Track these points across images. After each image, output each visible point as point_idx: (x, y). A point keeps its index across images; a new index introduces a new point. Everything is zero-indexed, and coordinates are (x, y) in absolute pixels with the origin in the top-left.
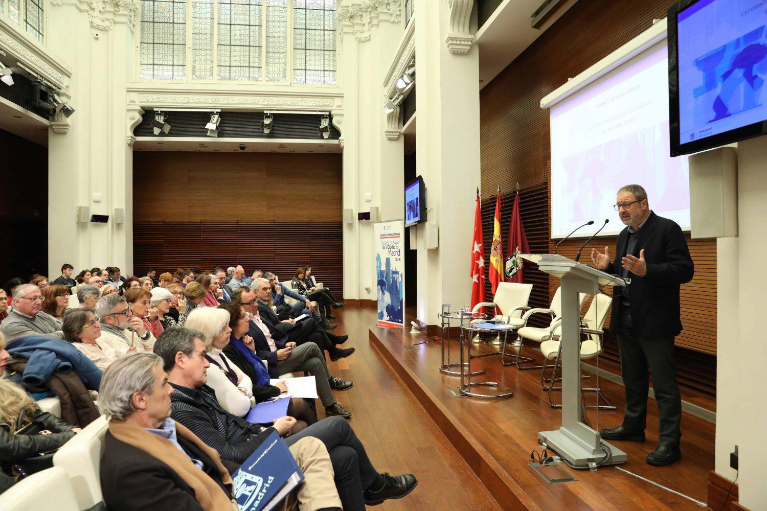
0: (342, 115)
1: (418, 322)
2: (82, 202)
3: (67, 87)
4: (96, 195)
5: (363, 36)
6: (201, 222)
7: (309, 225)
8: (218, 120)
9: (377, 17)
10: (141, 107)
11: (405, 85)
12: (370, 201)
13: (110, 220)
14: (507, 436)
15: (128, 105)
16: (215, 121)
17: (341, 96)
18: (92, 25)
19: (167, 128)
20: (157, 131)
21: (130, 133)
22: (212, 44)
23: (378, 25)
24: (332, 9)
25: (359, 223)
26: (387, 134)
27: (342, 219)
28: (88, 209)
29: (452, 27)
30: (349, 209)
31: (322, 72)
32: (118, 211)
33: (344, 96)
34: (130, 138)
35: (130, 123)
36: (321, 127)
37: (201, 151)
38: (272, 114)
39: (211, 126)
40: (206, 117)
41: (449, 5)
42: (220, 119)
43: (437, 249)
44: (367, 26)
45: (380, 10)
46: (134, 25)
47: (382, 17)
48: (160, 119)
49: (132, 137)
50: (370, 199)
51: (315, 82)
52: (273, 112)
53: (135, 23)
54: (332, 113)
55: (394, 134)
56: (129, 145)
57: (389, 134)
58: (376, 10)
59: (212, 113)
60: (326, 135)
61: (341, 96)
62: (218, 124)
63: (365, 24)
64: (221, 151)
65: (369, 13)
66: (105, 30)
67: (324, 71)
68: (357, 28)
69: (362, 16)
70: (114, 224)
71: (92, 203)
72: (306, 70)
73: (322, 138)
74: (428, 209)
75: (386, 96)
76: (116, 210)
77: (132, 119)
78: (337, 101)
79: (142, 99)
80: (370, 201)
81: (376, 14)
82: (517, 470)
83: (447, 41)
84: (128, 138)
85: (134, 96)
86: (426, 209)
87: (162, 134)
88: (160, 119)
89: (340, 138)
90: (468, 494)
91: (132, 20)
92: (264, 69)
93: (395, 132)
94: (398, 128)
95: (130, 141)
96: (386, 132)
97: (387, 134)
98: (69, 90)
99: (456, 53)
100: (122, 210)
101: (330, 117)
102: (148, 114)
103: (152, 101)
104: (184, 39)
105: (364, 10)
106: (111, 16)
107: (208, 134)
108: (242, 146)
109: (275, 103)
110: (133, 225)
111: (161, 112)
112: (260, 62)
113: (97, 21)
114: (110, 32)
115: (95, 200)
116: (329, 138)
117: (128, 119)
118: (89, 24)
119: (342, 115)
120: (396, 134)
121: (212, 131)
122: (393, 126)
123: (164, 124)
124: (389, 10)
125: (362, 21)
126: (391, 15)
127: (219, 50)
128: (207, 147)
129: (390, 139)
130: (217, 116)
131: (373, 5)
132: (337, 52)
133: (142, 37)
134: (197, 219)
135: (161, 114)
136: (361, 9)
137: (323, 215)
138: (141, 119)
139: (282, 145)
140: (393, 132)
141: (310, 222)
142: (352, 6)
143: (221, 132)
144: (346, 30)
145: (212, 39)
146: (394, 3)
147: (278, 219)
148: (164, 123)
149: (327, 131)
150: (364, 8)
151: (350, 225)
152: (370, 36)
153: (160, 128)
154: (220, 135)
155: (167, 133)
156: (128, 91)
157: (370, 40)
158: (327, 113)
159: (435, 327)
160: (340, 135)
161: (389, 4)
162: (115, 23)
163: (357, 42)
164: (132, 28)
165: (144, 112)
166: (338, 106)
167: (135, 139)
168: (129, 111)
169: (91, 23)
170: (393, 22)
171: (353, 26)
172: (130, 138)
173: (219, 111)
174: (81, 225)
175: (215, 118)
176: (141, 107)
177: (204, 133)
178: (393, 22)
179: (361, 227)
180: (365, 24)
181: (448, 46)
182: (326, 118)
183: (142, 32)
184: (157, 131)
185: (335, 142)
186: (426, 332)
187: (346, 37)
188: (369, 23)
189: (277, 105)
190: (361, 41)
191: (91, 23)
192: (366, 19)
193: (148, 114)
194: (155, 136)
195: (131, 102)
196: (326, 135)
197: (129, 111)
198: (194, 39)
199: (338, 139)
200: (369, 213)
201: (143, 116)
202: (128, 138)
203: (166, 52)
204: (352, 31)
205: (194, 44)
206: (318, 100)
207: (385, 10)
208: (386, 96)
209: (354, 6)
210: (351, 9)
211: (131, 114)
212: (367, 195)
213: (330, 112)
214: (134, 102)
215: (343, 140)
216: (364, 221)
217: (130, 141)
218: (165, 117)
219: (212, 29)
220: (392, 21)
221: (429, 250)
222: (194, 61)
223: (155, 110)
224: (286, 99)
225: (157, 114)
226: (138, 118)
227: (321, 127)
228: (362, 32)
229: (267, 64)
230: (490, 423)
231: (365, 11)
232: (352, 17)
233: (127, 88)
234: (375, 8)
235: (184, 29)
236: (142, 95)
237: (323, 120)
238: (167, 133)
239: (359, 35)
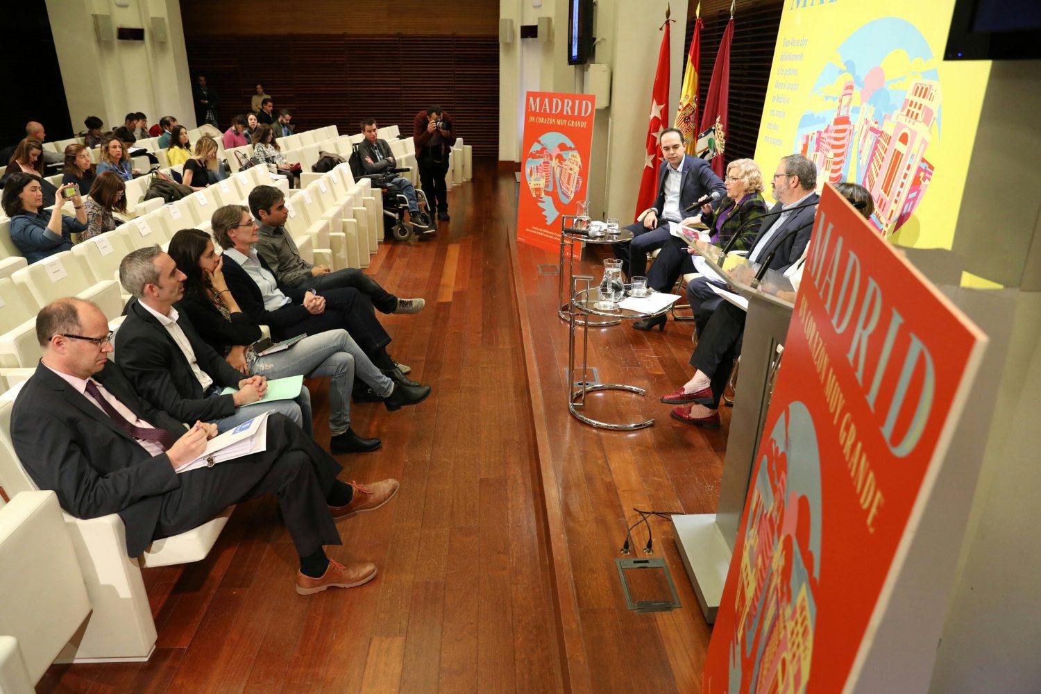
13: (147, 36)
14: (611, 488)
25: (523, 42)
28: (108, 18)
30: (506, 20)
32: (157, 21)
43: (608, 109)
71: (116, 9)
74: (598, 40)
80: (540, 6)
82: (592, 571)
86: (595, 39)
90: (517, 588)
100: (163, 19)
110: (186, 41)
134: (283, 30)
151: (510, 46)
216: (530, 40)
230: (598, 453)
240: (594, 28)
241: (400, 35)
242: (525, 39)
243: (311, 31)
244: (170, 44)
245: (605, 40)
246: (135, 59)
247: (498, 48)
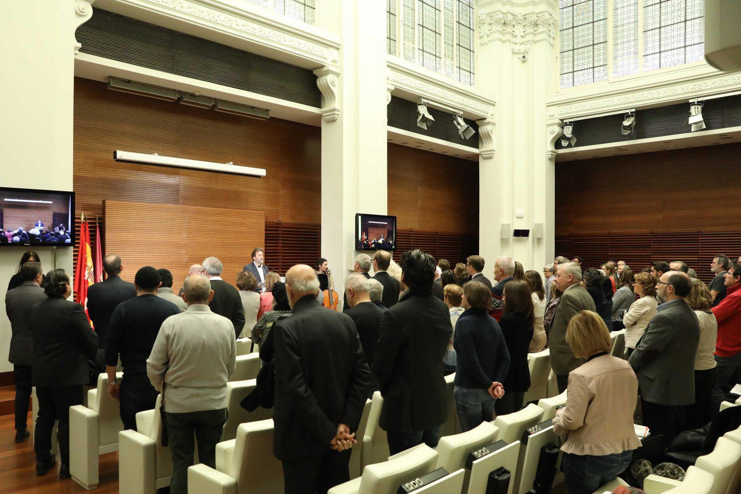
2: (505, 220)
3: (492, 115)
4: (519, 211)
15: (548, 120)
21: (551, 147)
32: (539, 226)
40: (622, 117)
46: (553, 38)
71: (516, 220)
76: (535, 224)
91: (551, 34)
98: (494, 117)
100: (542, 225)
145: (636, 28)
156: (547, 106)
162: (535, 42)
168: (548, 126)
173: (633, 110)
174: (504, 241)
197: (548, 126)
211: (551, 129)
214: (553, 116)
217: (550, 155)
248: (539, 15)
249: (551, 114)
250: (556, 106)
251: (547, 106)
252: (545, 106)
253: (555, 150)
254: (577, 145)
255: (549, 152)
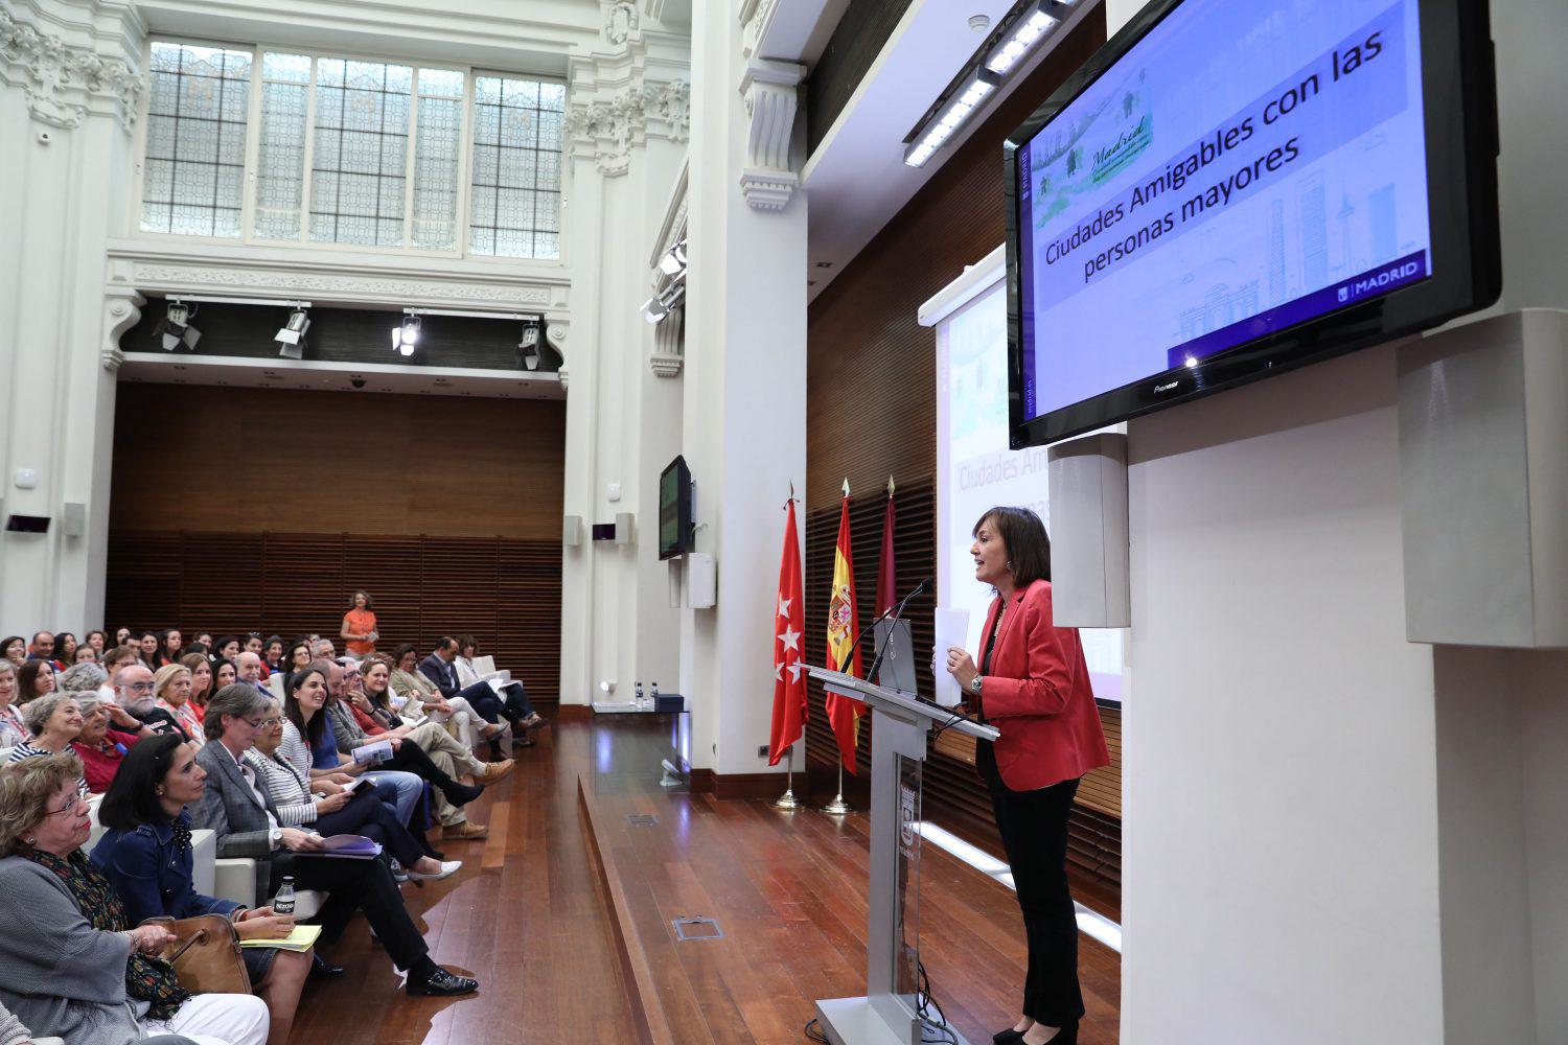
0: (566, 323)
1: (678, 762)
4: (24, 473)
5: (615, 165)
6: (266, 535)
7: (496, 546)
8: (303, 325)
9: (643, 129)
10: (139, 291)
11: (679, 268)
12: (618, 500)
13: (52, 528)
16: (297, 325)
17: (565, 284)
18: (33, 114)
19: (193, 337)
20: (169, 341)
21: (110, 345)
22: (300, 169)
23: (643, 145)
24: (555, 109)
25: (595, 545)
26: (655, 364)
27: (561, 535)
29: (752, 157)
31: (530, 235)
32: (74, 510)
33: (572, 283)
34: (111, 356)
35: (112, 323)
36: (521, 346)
37: (271, 386)
38: (419, 315)
39: (288, 336)
40: (281, 316)
41: (747, 111)
42: (308, 322)
43: (714, 609)
44: (623, 147)
45: (648, 114)
46: (132, 121)
47: (651, 129)
48: (179, 318)
49: (114, 353)
50: (616, 496)
51: (515, 251)
52: (421, 312)
53: (134, 117)
54: (546, 317)
55: (668, 364)
56: (108, 369)
57: (659, 364)
58: (642, 115)
59: (293, 310)
60: (531, 363)
61: (565, 284)
62: (303, 334)
63: (618, 142)
64: (314, 387)
65: (626, 120)
66: (64, 127)
67: (534, 231)
68: (602, 148)
69: (613, 125)
70: (64, 538)
71: (13, 491)
72: (495, 228)
73: (525, 368)
74: (697, 526)
75: (654, 287)
76: (68, 505)
77: (116, 315)
78: (558, 294)
79: (140, 274)
80: (618, 500)
81: (641, 122)
83: (743, 183)
84: (105, 355)
85: (123, 268)
86: (694, 524)
87: (181, 349)
88: (179, 318)
89: (560, 369)
91: (129, 110)
92: (408, 224)
93: (671, 361)
94: (679, 354)
95: (109, 361)
96: (653, 360)
97: (655, 364)
99: (760, 209)
100: (82, 506)
101: (542, 325)
102: (153, 306)
103: (161, 279)
104: (241, 155)
105: (617, 113)
106: (79, 99)
107: (282, 353)
108: (358, 380)
109: (426, 294)
111: (182, 302)
112: (401, 208)
113: (45, 108)
114: (75, 133)
115: (20, 482)
116: (537, 370)
117: (108, 316)
118: (26, 114)
119: (566, 323)
120: (673, 365)
121: (290, 346)
122: (668, 347)
123: (186, 328)
124: (667, 116)
125: (613, 134)
126: (671, 125)
127: (315, 181)
128: (279, 378)
129: (660, 376)
130: (301, 316)
131: (634, 105)
132: (563, 197)
133: (150, 145)
134: (258, 528)
135: (181, 308)
136: (611, 111)
137: (521, 527)
138: (138, 315)
139: (442, 381)
140: (666, 361)
141: (499, 540)
142: (595, 103)
143: (310, 347)
144: (580, 151)
145: (301, 159)
146: (677, 103)
147: (429, 534)
148: (185, 326)
149: (535, 354)
150: (617, 109)
151: (577, 550)
152: (627, 165)
153: (178, 336)
154: (307, 356)
155: (192, 347)
156: (110, 256)
157: (627, 174)
158: (536, 318)
159: (708, 773)
160: (561, 363)
161: (667, 103)
162: (89, 113)
163: (601, 176)
164: (128, 127)
165: (144, 302)
166: (557, 305)
167: (120, 357)
168: (110, 297)
169: (33, 110)
170: (675, 141)
171: (595, 144)
172: (111, 356)
173: (308, 305)
175: (298, 320)
176: (138, 291)
177: (274, 350)
178: (675, 141)
179: (598, 554)
180: (618, 142)
181: (745, 194)
182: (533, 327)
183: (151, 135)
184: (169, 341)
185: (550, 376)
186: (688, 783)
187: (580, 166)
188: (627, 140)
189: (432, 298)
190: (610, 176)
191: (33, 110)
192: (621, 132)
193: (153, 306)
194: (167, 352)
195: (116, 278)
196: (531, 363)
197: (110, 297)
198: (263, 156)
199: (556, 371)
200: (613, 526)
201: (142, 309)
202: (105, 355)
203: (201, 179)
204: (593, 155)
205: (262, 165)
206: (519, 290)
207: (659, 116)
208: (654, 287)
209: (598, 106)
210: (590, 111)
211: (116, 305)
212: (613, 487)
213: (542, 316)
214: (123, 279)
215: (567, 374)
216: (605, 542)
217: (109, 361)
218: (190, 313)
219: (302, 137)
220: (672, 136)
221: (699, 612)
222: (260, 201)
223: (169, 297)
224: (452, 286)
225: (175, 307)
226: (129, 312)
227: (521, 346)
228: (613, 157)
229: (416, 213)
231: (619, 116)
232: (593, 126)
233: (109, 250)
234: (639, 111)
235: (243, 135)
236: (140, 267)
237: (527, 331)
238: (192, 347)
239: (606, 162)
240: (692, 512)
241: (422, 537)
242: (599, 541)
243: (301, 529)
244: (86, 541)
245: (706, 525)
246: (32, 557)
247: (561, 555)
248: (105, 61)
249: (118, 274)
250: (131, 262)
251: (110, 256)
252: (103, 255)
253: (120, 352)
254: (200, 349)
255: (107, 352)
